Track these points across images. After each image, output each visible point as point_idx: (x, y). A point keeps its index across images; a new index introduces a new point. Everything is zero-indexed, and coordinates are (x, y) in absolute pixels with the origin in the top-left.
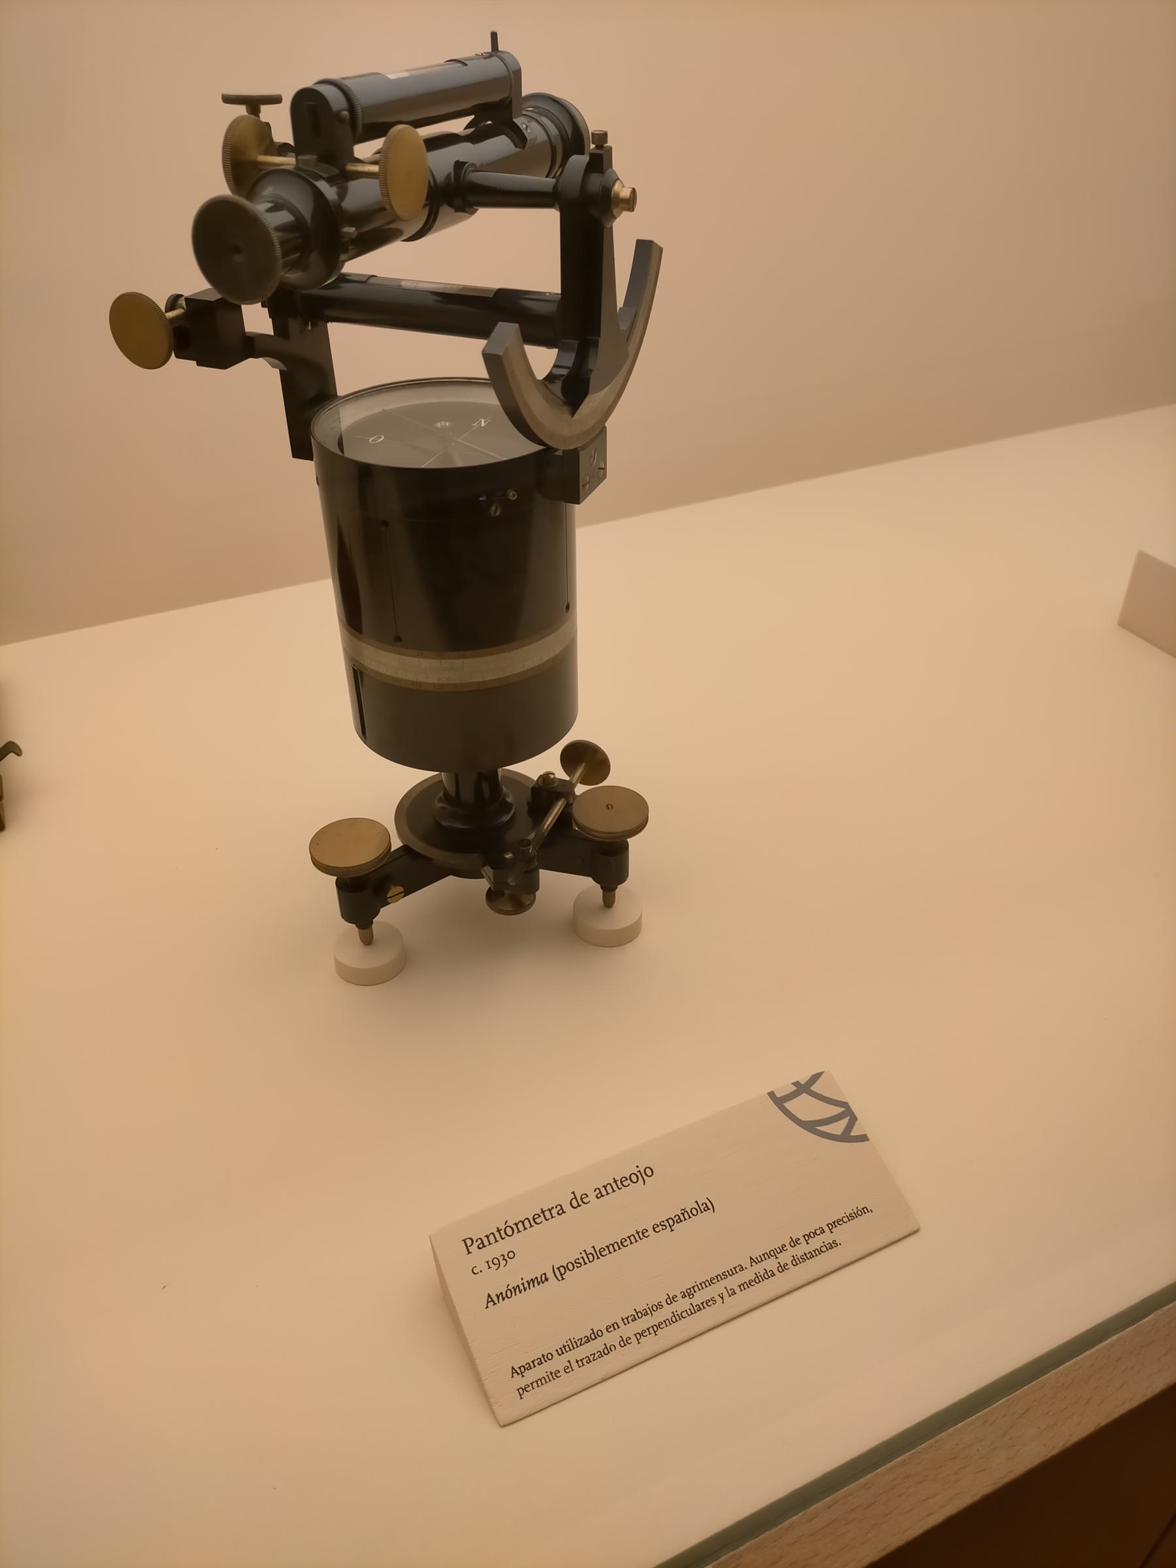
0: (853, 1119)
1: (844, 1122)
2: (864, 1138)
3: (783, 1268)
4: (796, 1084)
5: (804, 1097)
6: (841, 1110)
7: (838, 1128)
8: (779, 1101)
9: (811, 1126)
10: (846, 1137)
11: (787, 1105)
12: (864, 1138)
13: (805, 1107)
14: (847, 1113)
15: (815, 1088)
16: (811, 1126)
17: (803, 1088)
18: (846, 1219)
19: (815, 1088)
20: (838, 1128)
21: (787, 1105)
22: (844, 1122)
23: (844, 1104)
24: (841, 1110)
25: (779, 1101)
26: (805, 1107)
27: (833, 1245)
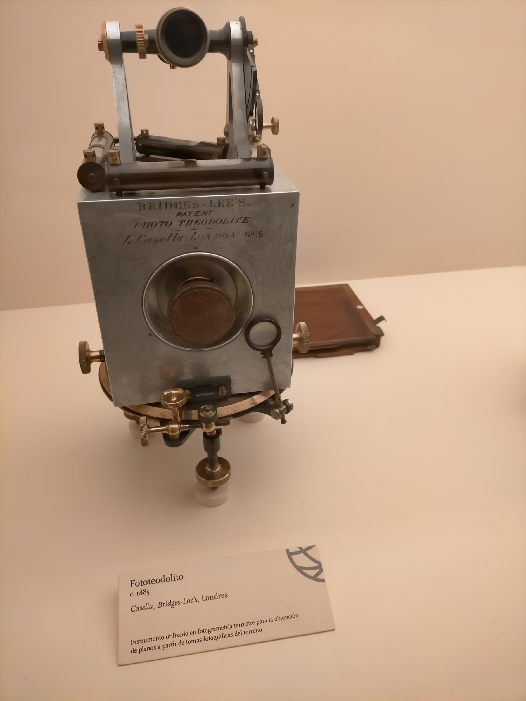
0: (321, 571)
1: (317, 571)
2: (323, 581)
3: (181, 643)
4: (300, 548)
5: (302, 555)
6: (316, 565)
7: (312, 573)
8: (290, 554)
9: (300, 569)
10: (315, 578)
11: (293, 557)
12: (323, 581)
13: (301, 560)
14: (320, 567)
15: (308, 552)
16: (300, 569)
17: (303, 551)
18: (290, 617)
19: (308, 552)
20: (312, 573)
21: (293, 557)
22: (317, 571)
23: (320, 563)
24: (316, 565)
25: (290, 554)
26: (301, 560)
27: (260, 630)
